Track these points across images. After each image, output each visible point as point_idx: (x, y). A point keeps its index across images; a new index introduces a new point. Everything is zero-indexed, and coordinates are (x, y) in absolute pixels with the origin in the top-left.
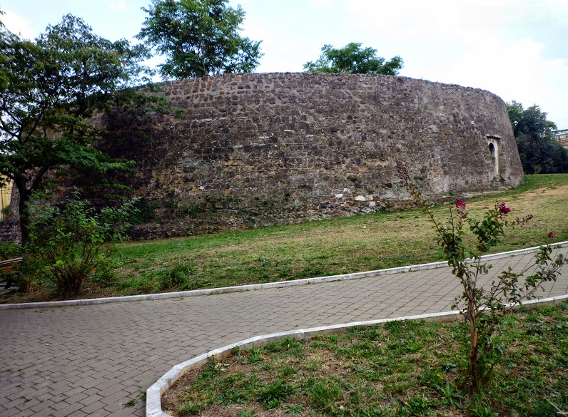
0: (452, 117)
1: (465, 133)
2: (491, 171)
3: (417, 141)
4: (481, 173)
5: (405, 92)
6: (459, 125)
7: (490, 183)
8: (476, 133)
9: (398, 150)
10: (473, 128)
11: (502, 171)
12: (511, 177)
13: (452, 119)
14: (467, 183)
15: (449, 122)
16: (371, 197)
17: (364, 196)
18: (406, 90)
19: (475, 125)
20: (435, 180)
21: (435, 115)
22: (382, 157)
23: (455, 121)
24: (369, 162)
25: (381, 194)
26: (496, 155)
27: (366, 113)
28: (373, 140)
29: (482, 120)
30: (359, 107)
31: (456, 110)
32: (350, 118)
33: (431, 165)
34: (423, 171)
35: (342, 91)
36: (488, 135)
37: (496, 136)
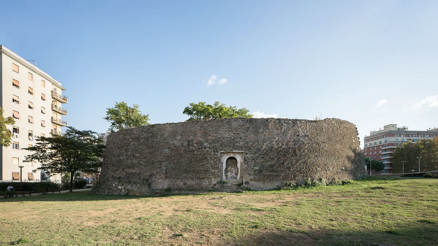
0: (186, 142)
1: (195, 152)
2: (215, 177)
3: (152, 159)
4: (204, 178)
5: (153, 132)
6: (191, 147)
7: (211, 186)
8: (207, 151)
9: (141, 164)
10: (205, 148)
11: (241, 177)
12: (251, 183)
13: (186, 143)
14: (185, 184)
15: (183, 146)
16: (123, 187)
17: (121, 186)
18: (155, 131)
19: (209, 146)
20: (158, 181)
21: (171, 143)
22: (132, 167)
23: (189, 145)
24: (127, 170)
25: (126, 186)
26: (239, 165)
27: (132, 146)
28: (131, 159)
29: (218, 142)
30: (131, 143)
31: (192, 137)
32: (126, 149)
33: (157, 173)
34: (150, 176)
35: (127, 137)
36: (223, 152)
37: (237, 151)
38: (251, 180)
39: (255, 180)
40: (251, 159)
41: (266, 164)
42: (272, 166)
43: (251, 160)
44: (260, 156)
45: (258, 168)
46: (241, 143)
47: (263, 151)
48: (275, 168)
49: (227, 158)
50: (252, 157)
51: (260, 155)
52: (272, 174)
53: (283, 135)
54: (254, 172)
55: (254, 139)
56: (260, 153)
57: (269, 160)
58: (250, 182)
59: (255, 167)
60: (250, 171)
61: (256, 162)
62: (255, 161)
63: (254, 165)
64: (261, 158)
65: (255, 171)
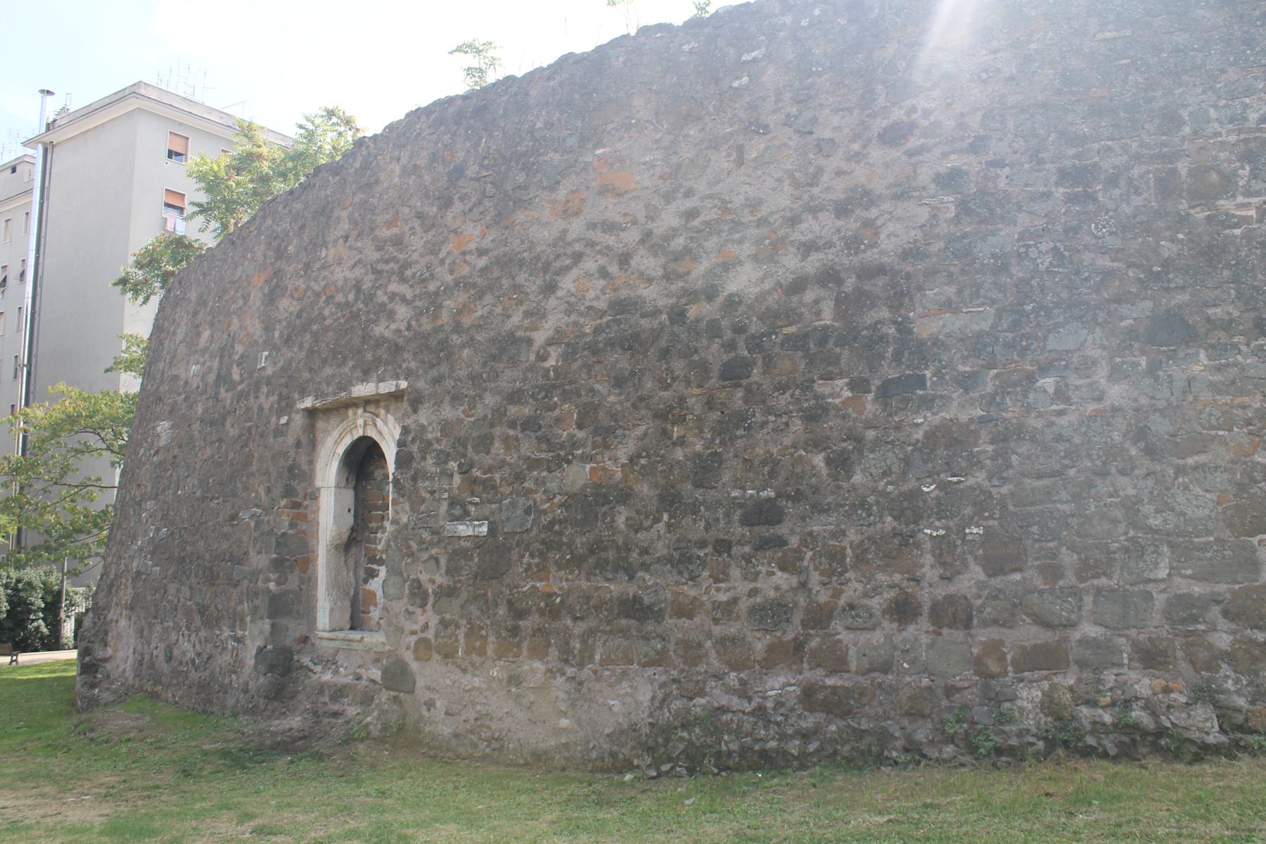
38: (423, 650)
39: (448, 655)
40: (444, 445)
41: (553, 486)
42: (594, 502)
43: (443, 458)
44: (513, 410)
45: (485, 529)
46: (403, 312)
47: (542, 358)
48: (621, 521)
49: (341, 450)
50: (446, 427)
51: (515, 397)
52: (584, 584)
53: (740, 162)
54: (448, 572)
55: (482, 262)
56: (509, 378)
57: (575, 444)
58: (414, 666)
59: (464, 516)
60: (425, 556)
61: (476, 473)
62: (465, 471)
63: (453, 503)
64: (512, 425)
65: (459, 555)
